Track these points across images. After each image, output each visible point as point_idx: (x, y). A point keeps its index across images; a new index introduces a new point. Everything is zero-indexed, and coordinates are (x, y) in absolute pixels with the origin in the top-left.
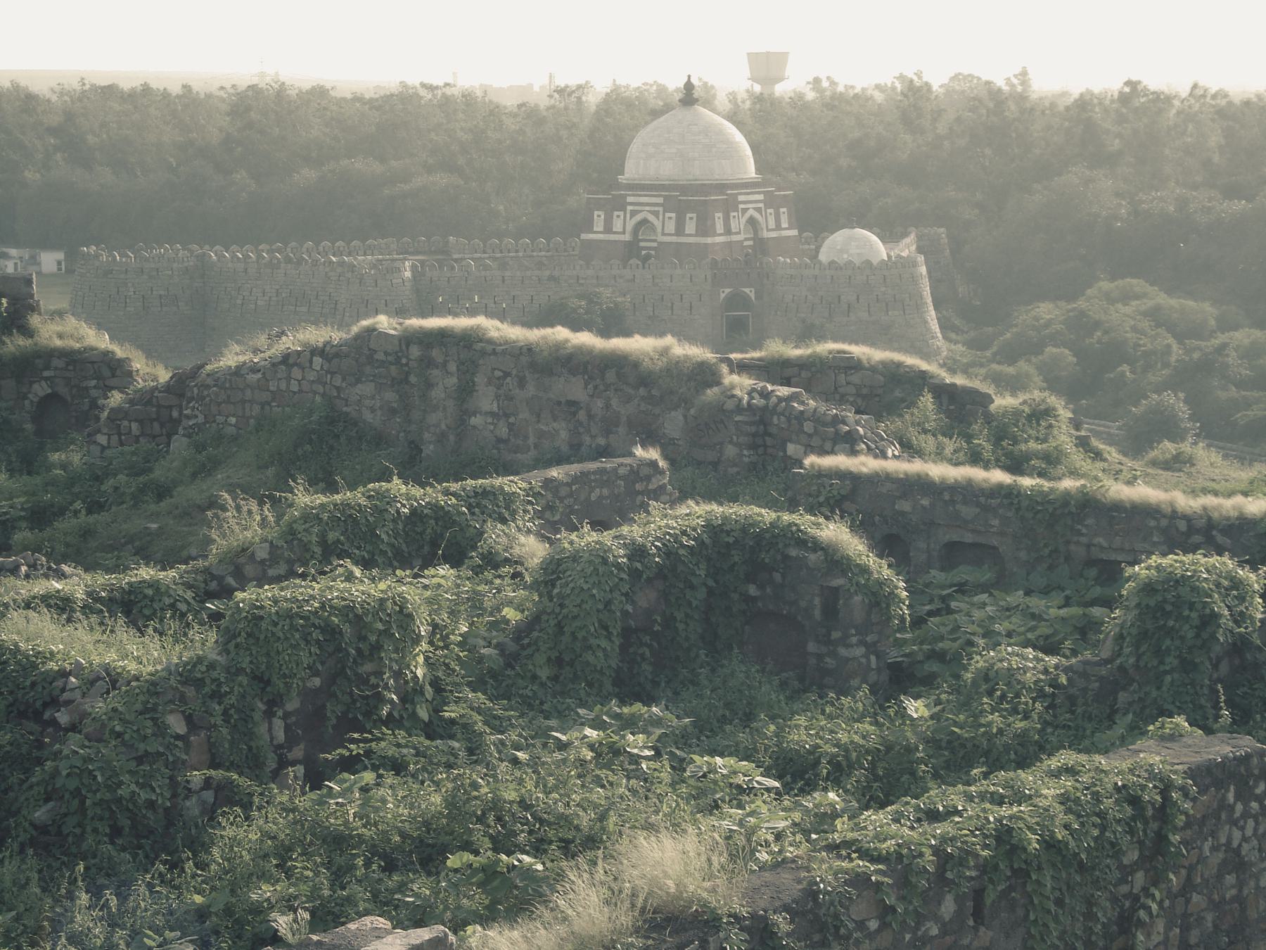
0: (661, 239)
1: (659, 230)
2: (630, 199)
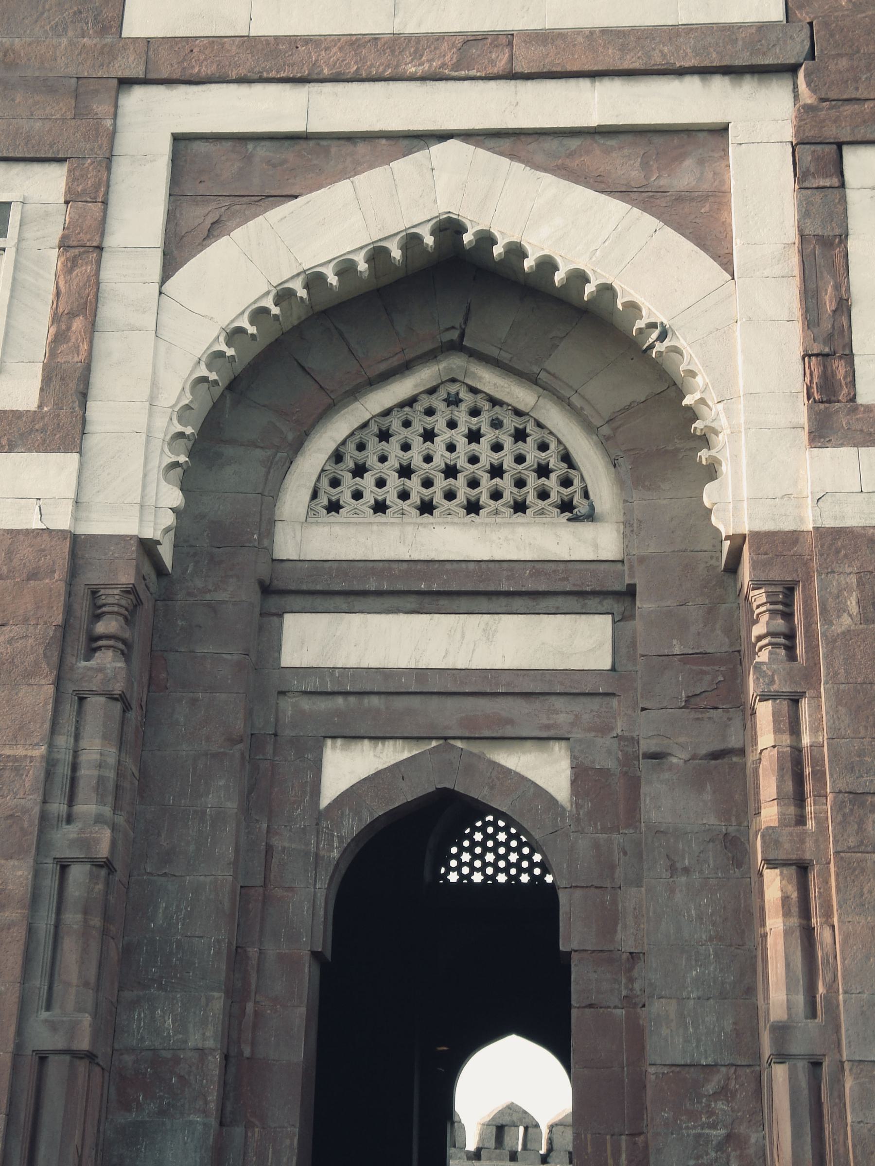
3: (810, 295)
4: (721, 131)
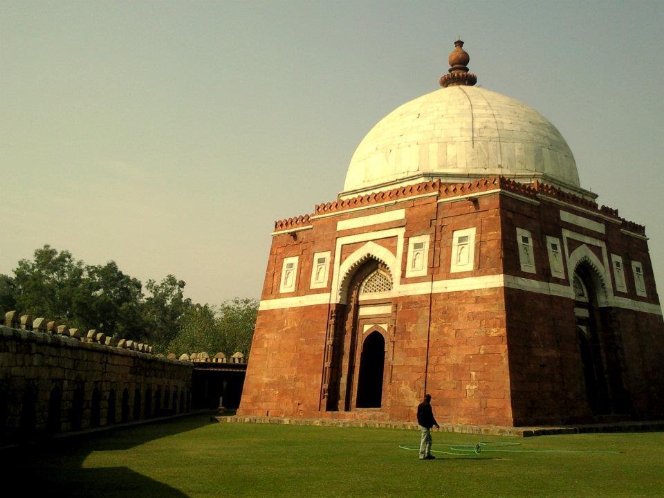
0: (399, 290)
1: (396, 273)
2: (341, 225)
3: (403, 262)
4: (397, 236)
